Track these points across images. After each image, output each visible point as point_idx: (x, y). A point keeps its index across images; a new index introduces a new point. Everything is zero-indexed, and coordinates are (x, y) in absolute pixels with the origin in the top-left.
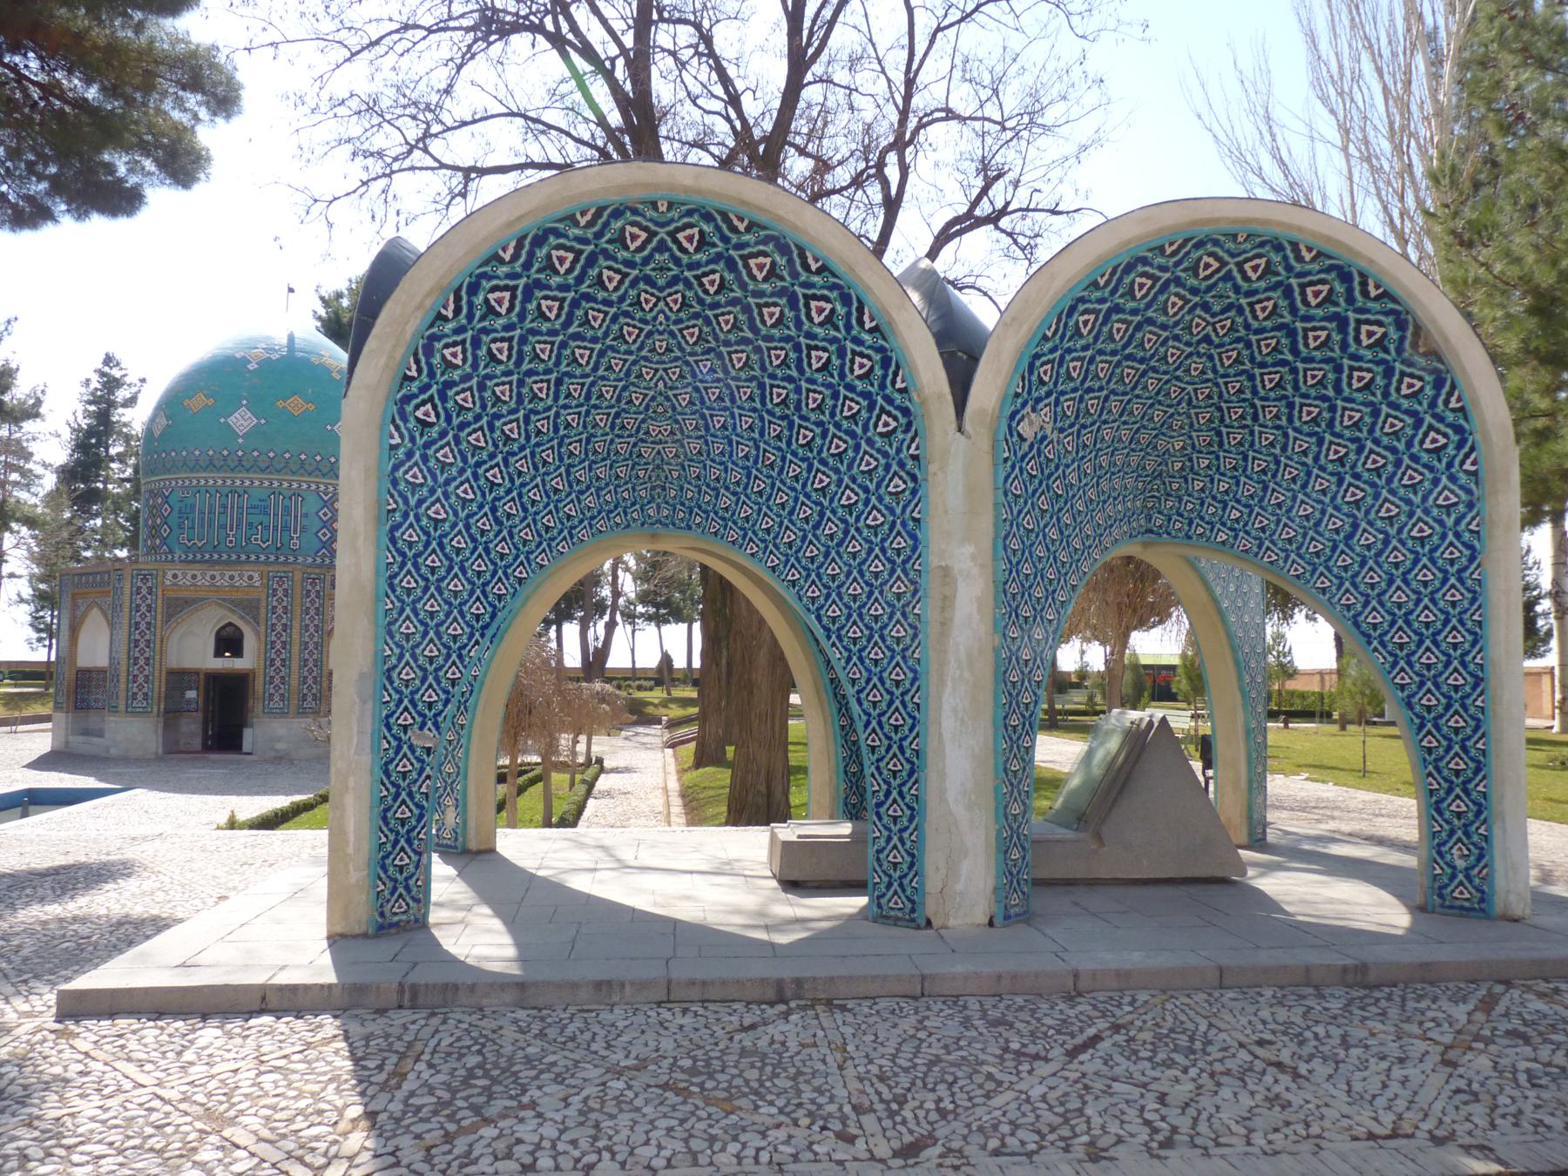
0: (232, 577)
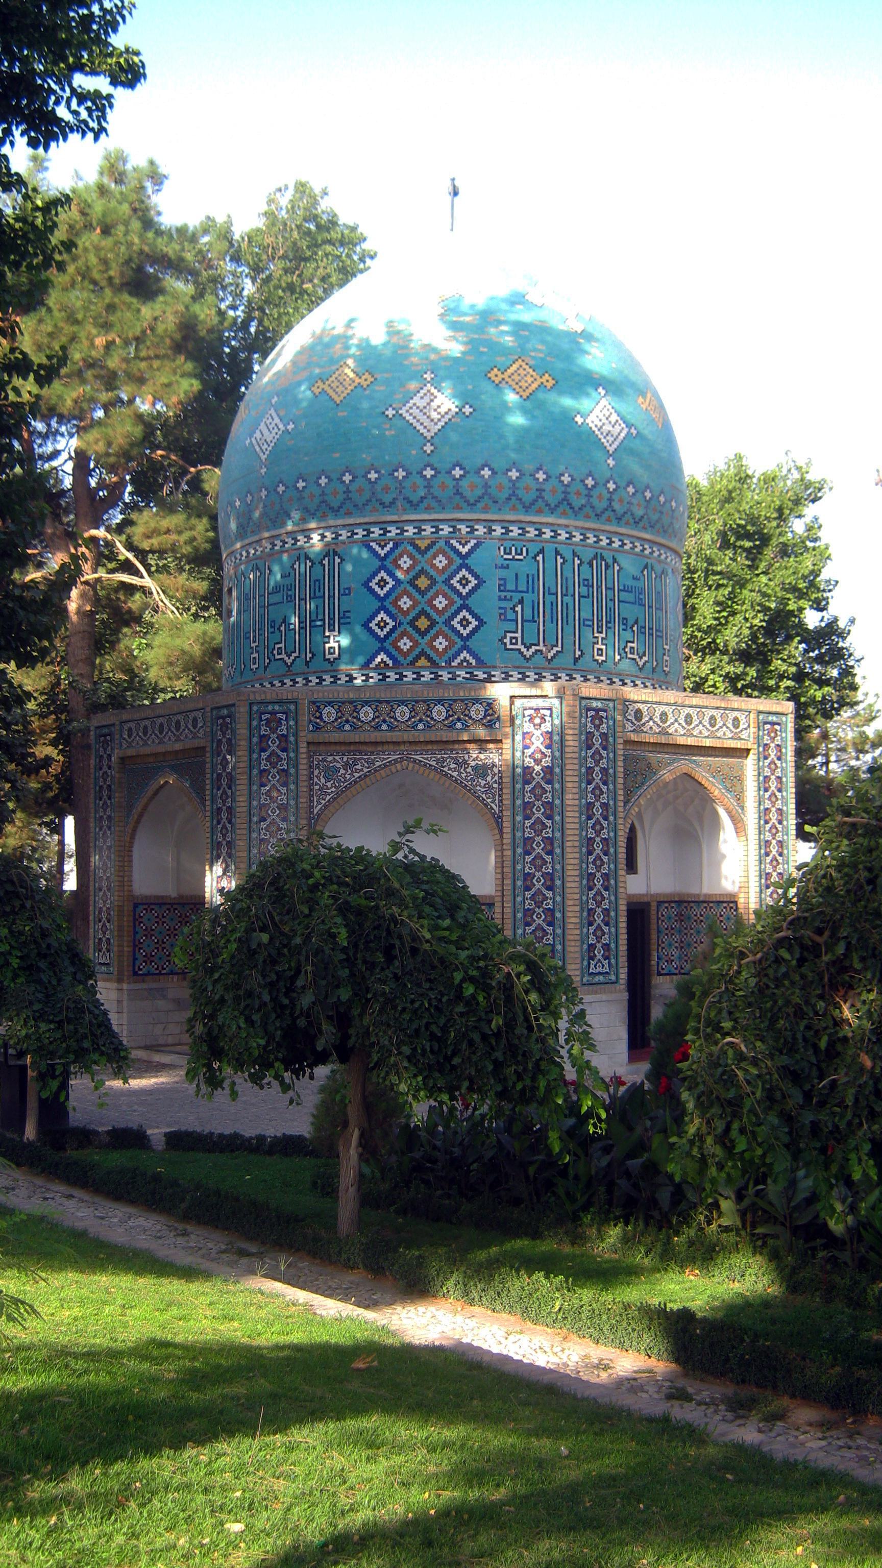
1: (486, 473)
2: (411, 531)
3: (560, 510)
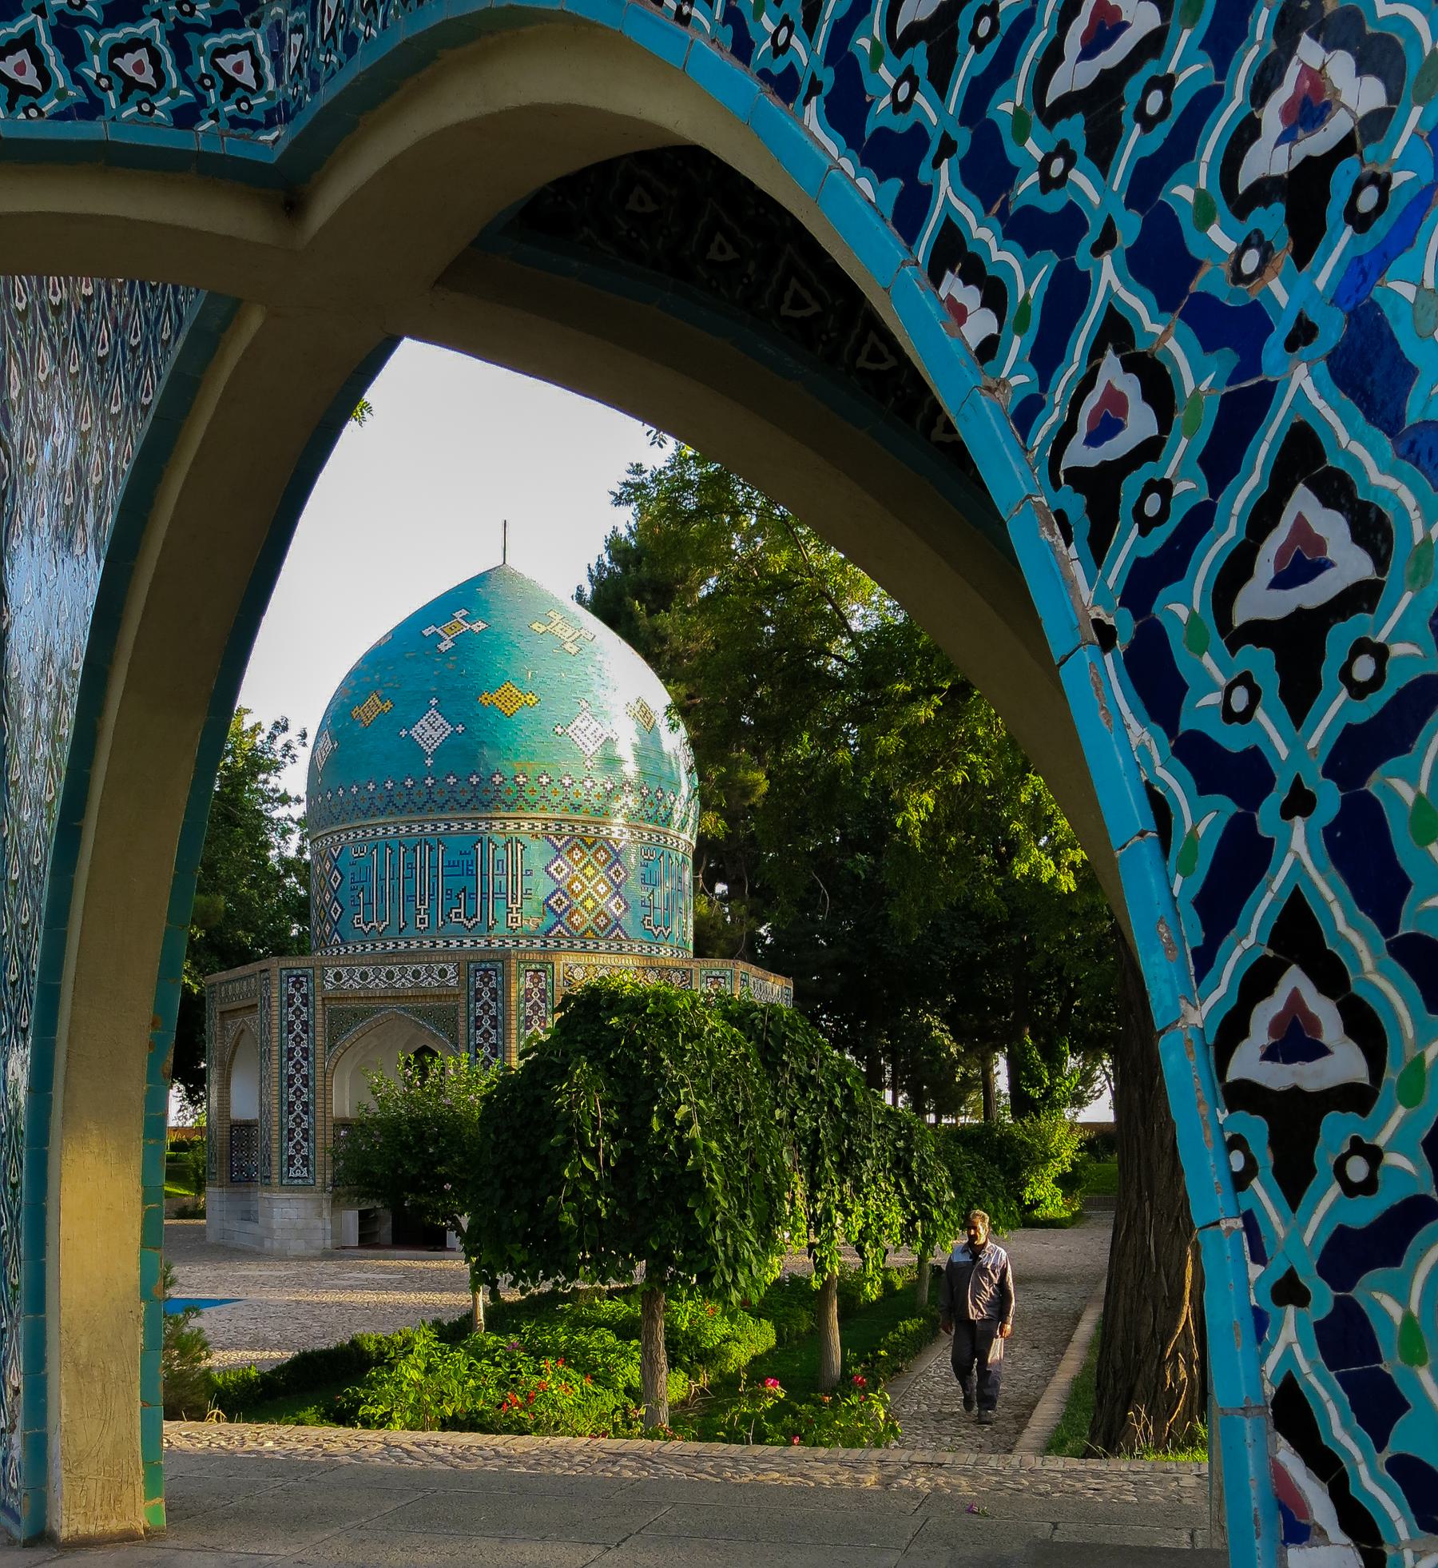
1: (341, 792)
3: (388, 811)
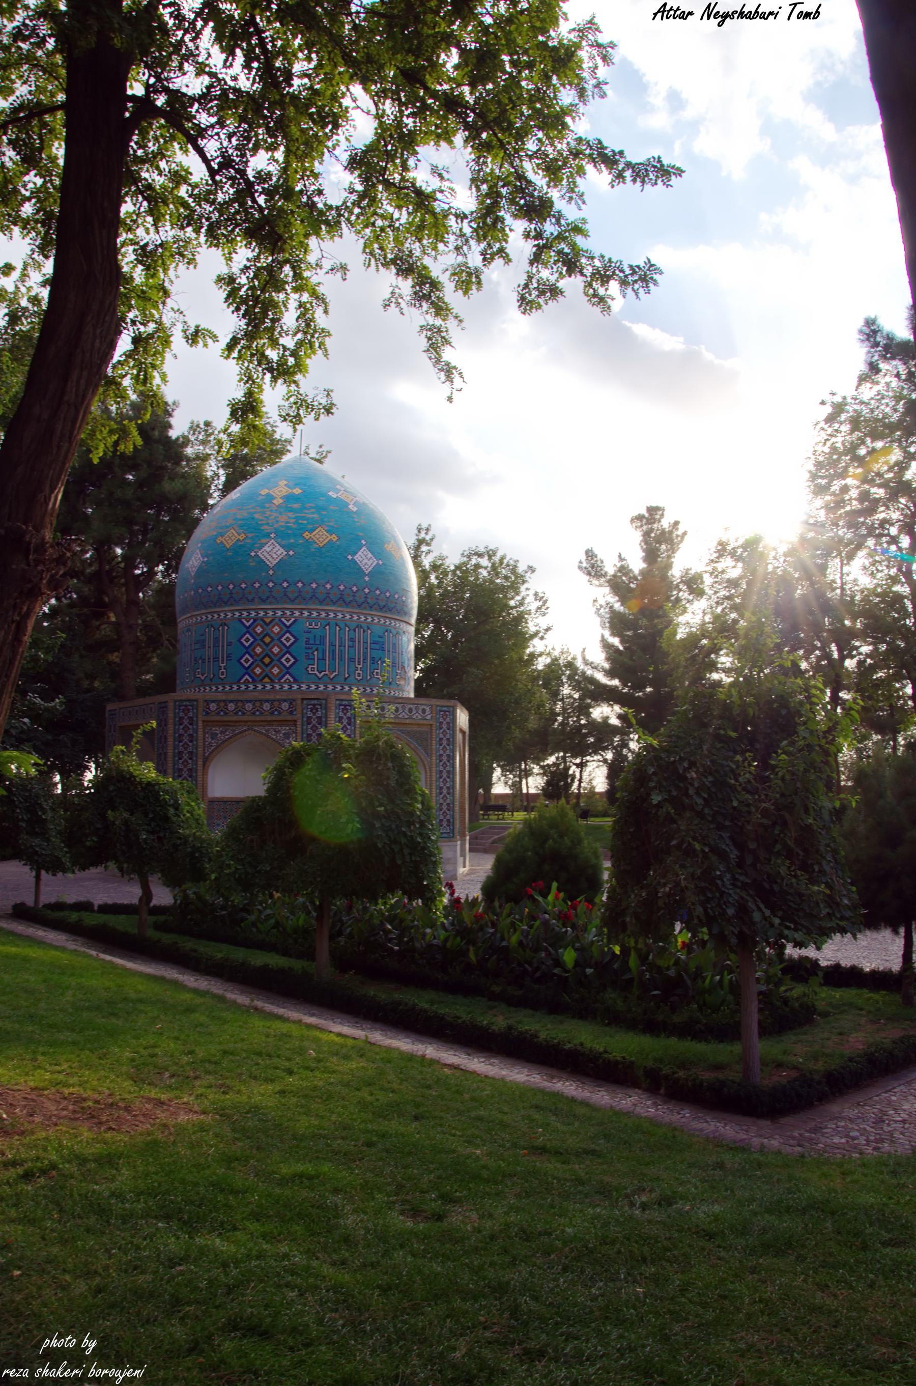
0: (410, 710)
1: (300, 585)
2: (262, 614)
